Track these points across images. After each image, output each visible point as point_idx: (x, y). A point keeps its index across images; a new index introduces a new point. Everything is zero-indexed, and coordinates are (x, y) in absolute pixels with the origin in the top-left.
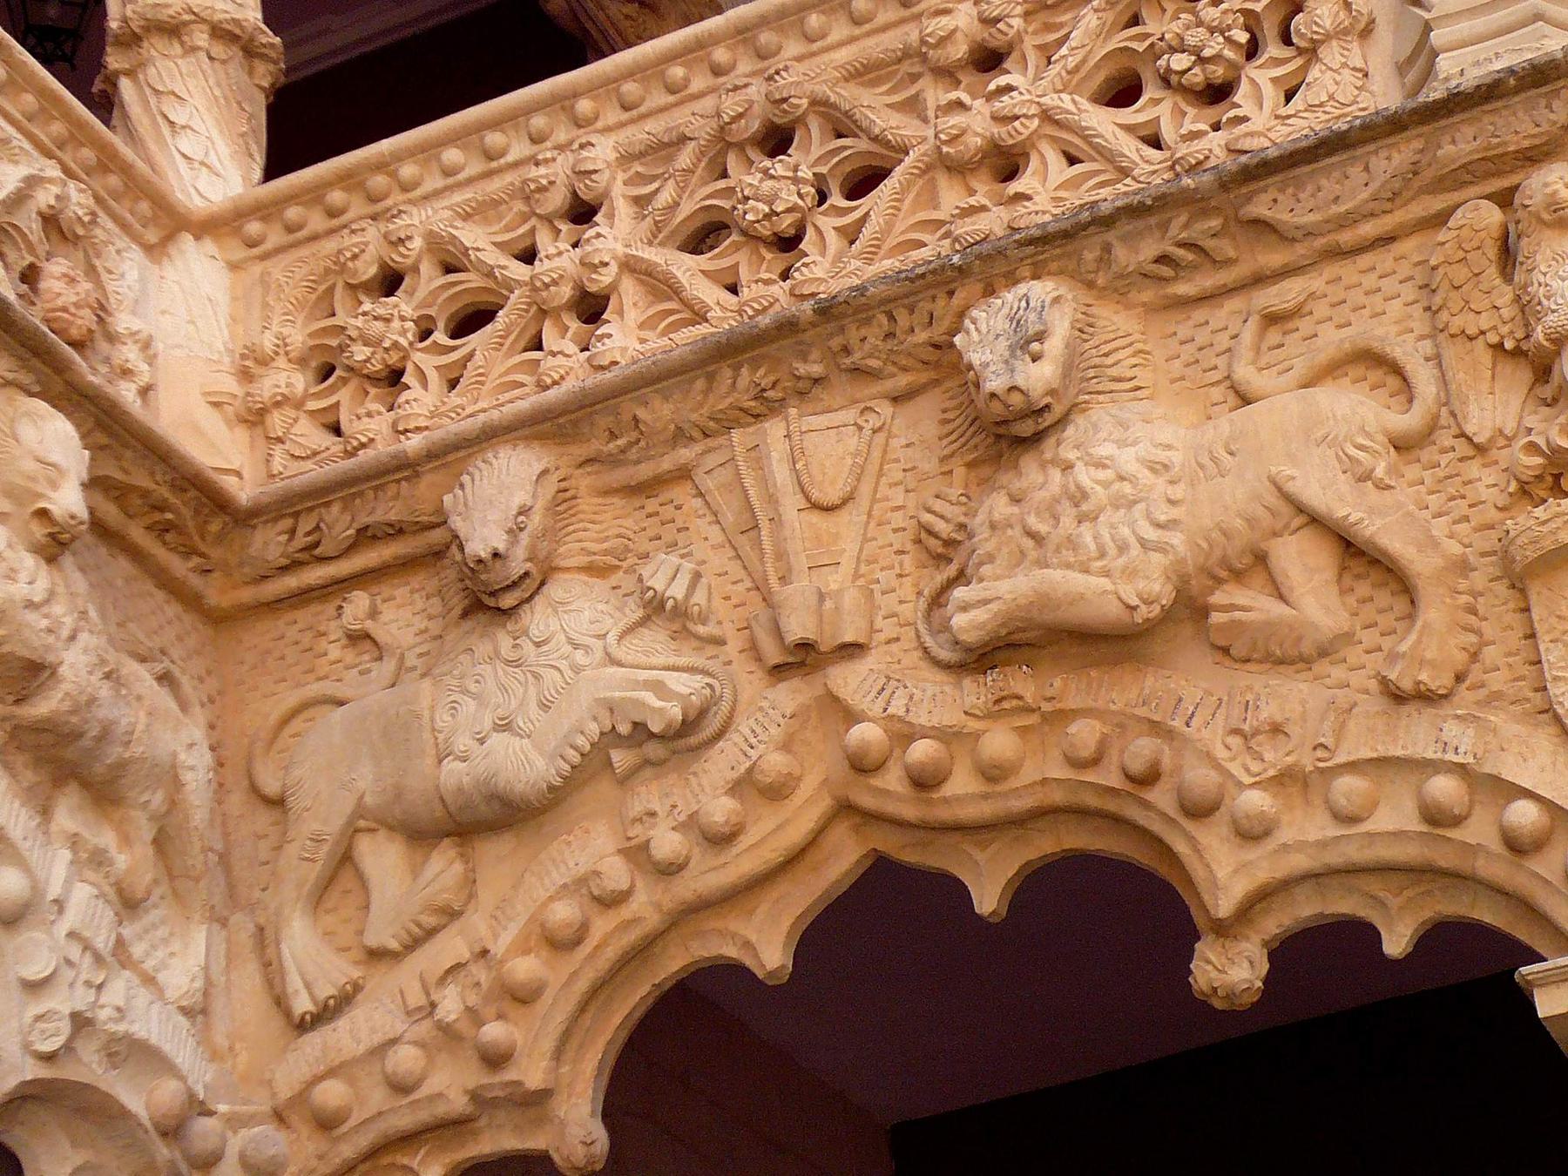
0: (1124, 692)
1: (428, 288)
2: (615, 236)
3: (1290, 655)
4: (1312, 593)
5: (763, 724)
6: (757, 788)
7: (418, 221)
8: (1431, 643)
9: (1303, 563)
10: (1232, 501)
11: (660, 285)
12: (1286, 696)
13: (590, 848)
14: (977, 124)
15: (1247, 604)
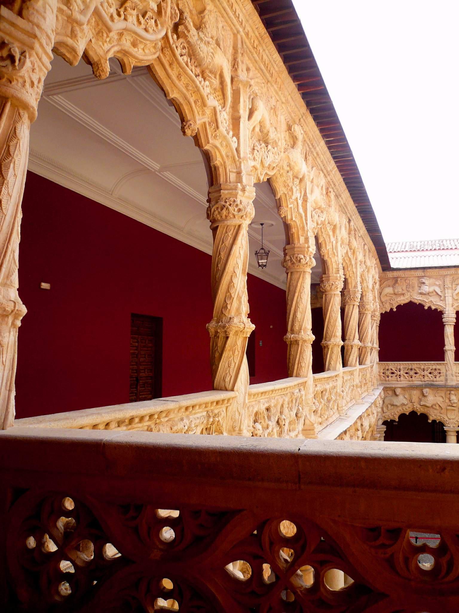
0: (428, 409)
1: (390, 371)
2: (402, 372)
3: (435, 409)
4: (438, 407)
5: (410, 405)
6: (409, 408)
7: (390, 367)
8: (442, 411)
9: (437, 406)
10: (435, 402)
11: (404, 376)
12: (435, 411)
13: (400, 408)
14: (423, 373)
15: (434, 407)
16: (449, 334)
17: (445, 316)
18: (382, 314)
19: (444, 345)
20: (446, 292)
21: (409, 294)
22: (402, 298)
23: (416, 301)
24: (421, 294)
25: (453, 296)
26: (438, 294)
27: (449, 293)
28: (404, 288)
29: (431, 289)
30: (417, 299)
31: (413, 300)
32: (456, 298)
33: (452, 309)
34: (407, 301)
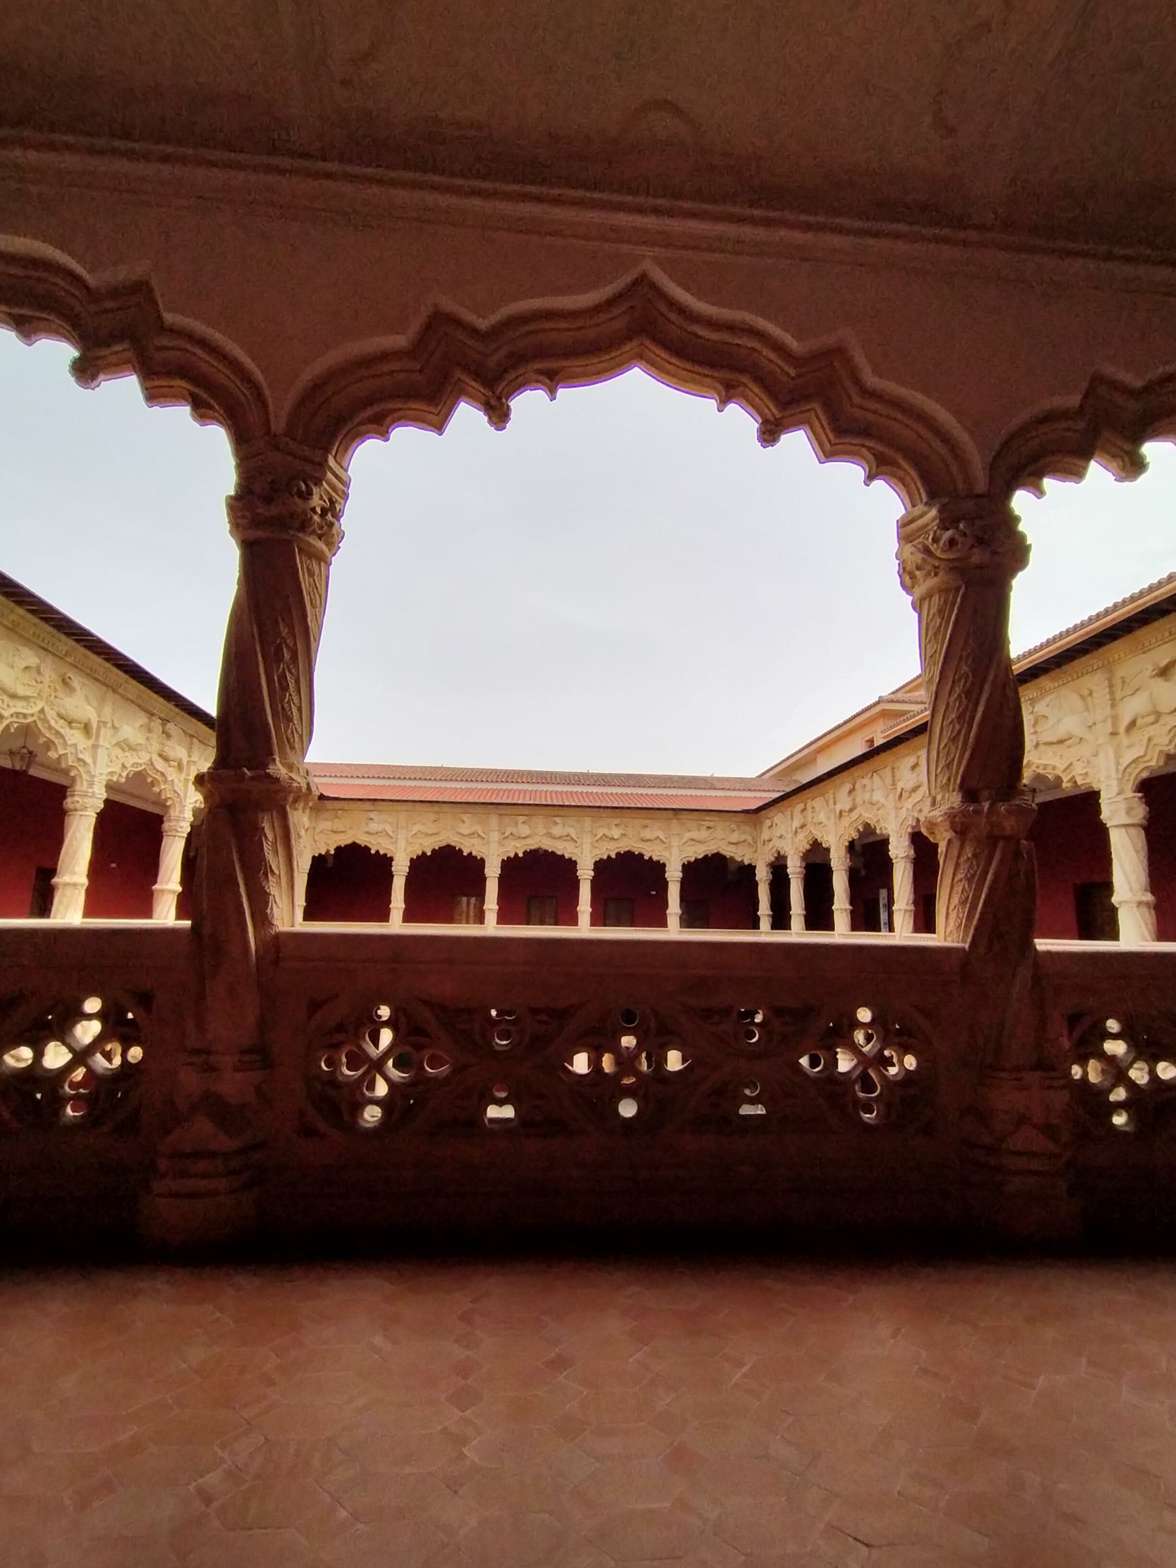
18: (314, 857)
19: (390, 902)
24: (368, 833)
29: (380, 829)
30: (362, 840)
32: (411, 840)
34: (349, 842)
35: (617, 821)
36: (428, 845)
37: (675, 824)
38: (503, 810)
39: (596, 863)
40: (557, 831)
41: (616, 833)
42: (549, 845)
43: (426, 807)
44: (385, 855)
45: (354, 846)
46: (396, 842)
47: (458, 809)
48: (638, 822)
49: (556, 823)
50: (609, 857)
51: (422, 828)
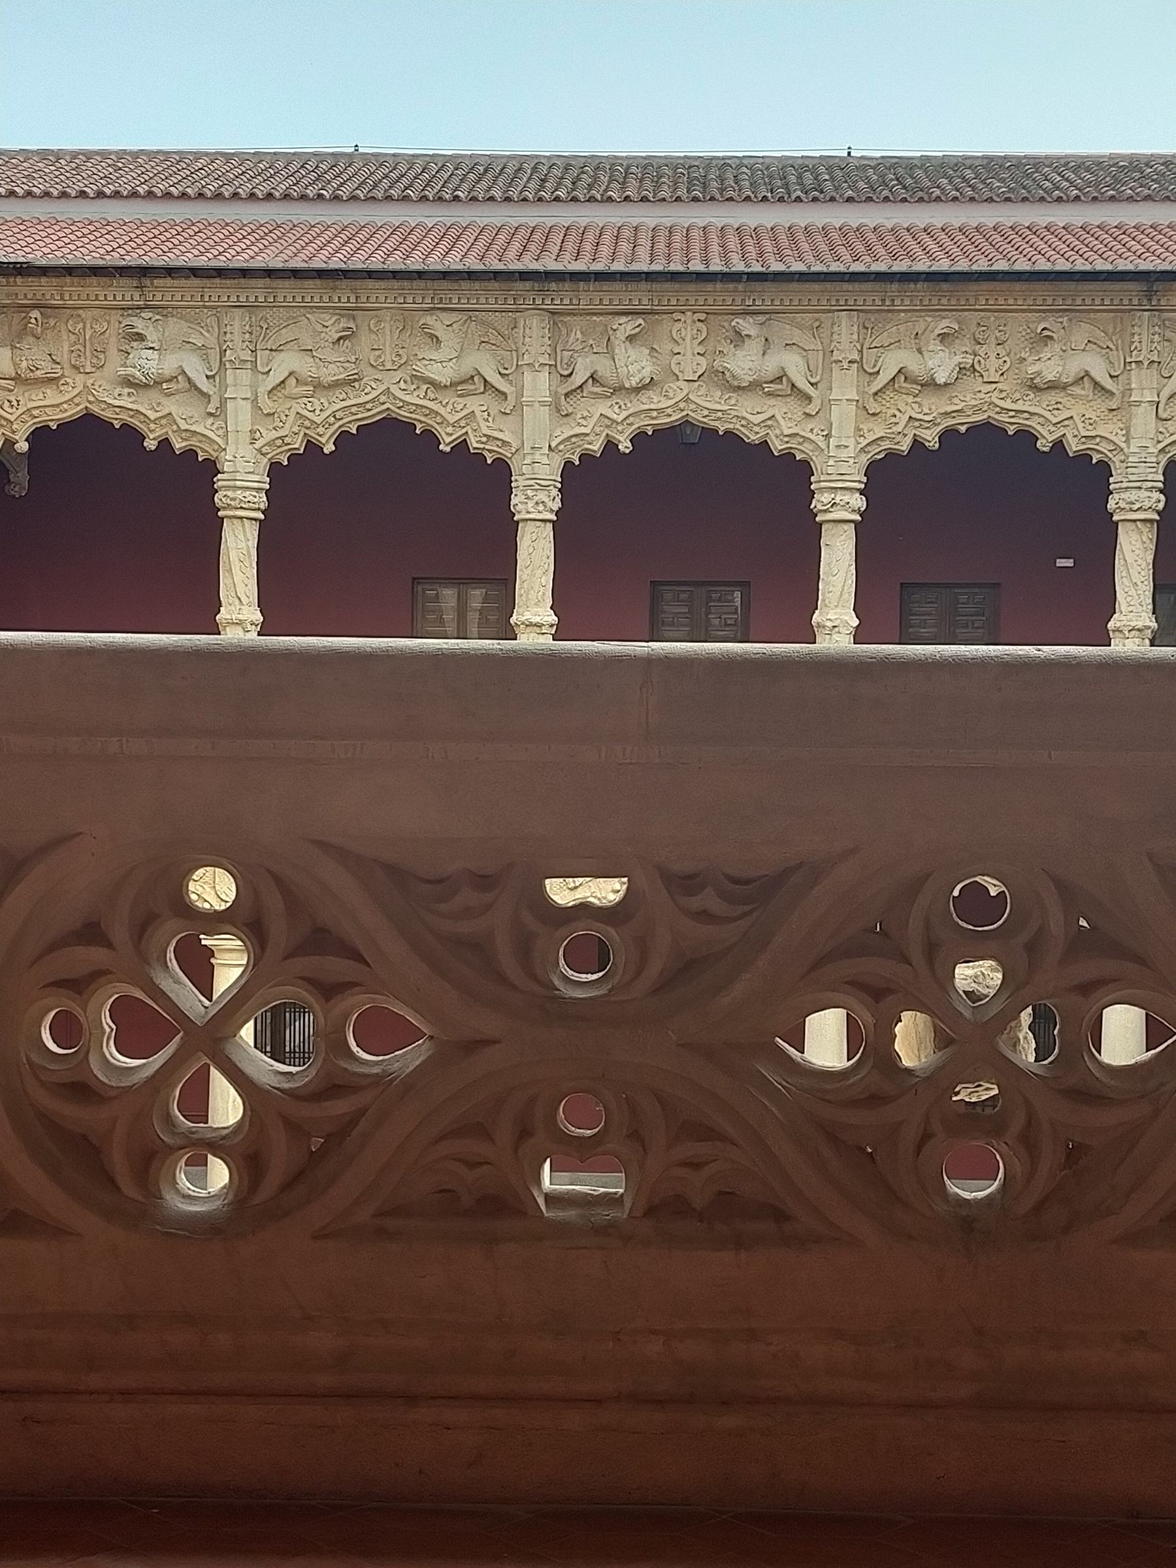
16: (233, 555)
17: (220, 481)
20: (229, 380)
21: (80, 378)
22: (52, 396)
23: (108, 414)
24: (128, 382)
25: (255, 400)
26: (197, 388)
27: (239, 384)
28: (63, 355)
29: (169, 364)
30: (115, 403)
31: (96, 409)
32: (267, 405)
33: (248, 452)
34: (71, 412)
35: (942, 326)
36: (326, 419)
37: (1145, 337)
38: (562, 296)
39: (873, 470)
40: (743, 363)
41: (941, 364)
42: (714, 409)
43: (312, 290)
44: (191, 453)
45: (89, 424)
46: (219, 414)
47: (416, 296)
48: (1018, 327)
49: (739, 338)
50: (917, 443)
51: (305, 366)
